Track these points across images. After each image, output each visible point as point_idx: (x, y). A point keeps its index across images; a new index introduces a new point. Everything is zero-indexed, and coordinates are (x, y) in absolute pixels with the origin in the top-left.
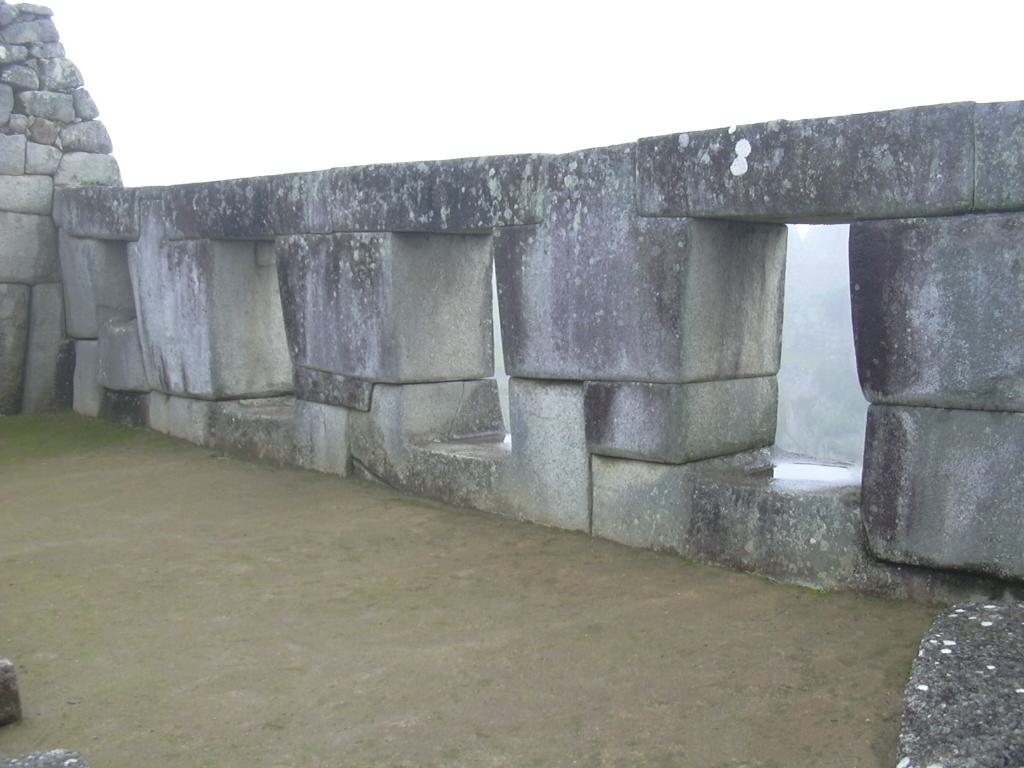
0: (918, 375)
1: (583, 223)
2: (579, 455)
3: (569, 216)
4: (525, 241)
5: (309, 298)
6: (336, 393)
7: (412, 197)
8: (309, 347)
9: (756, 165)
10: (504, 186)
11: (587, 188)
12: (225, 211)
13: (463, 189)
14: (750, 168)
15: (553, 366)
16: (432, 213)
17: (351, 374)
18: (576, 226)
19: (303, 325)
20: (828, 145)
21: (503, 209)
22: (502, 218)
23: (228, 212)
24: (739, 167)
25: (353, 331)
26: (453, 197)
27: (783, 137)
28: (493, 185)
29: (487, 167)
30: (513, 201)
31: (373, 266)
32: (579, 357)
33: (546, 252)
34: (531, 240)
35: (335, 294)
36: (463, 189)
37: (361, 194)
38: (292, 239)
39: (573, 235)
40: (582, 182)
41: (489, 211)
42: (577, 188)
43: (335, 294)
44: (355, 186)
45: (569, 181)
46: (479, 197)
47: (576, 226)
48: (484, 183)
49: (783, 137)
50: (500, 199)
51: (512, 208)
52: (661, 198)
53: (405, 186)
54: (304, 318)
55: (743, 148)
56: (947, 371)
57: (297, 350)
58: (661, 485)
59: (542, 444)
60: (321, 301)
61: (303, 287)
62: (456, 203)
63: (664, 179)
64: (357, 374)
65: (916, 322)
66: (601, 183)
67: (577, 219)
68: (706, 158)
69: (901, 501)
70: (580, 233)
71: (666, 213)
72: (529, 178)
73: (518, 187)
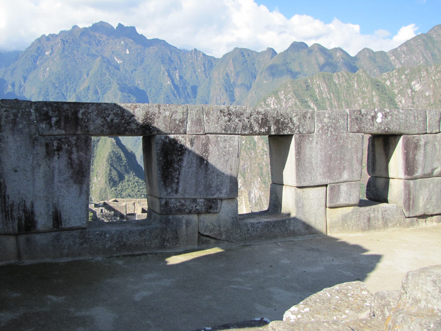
0: (417, 171)
1: (331, 134)
3: (326, 131)
4: (308, 139)
5: (185, 163)
6: (198, 207)
7: (256, 120)
8: (180, 189)
9: (383, 120)
10: (299, 119)
11: (333, 123)
12: (112, 120)
13: (282, 120)
15: (320, 180)
16: (267, 128)
17: (211, 197)
18: (329, 135)
19: (178, 178)
20: (401, 117)
21: (299, 128)
22: (299, 131)
23: (116, 121)
24: (379, 120)
26: (277, 122)
27: (390, 113)
28: (295, 119)
29: (292, 112)
30: (303, 125)
31: (231, 149)
32: (329, 177)
33: (317, 143)
34: (311, 139)
36: (282, 120)
37: (226, 118)
40: (331, 121)
41: (293, 128)
42: (329, 123)
44: (222, 114)
45: (326, 120)
46: (289, 123)
47: (329, 135)
48: (291, 119)
49: (390, 113)
50: (298, 124)
51: (303, 127)
52: (357, 127)
53: (252, 117)
54: (179, 174)
56: (423, 170)
57: (170, 190)
58: (352, 212)
59: (310, 208)
60: (195, 165)
61: (181, 160)
62: (279, 124)
63: (358, 122)
64: (215, 196)
65: (417, 159)
66: (338, 121)
68: (369, 117)
69: (411, 202)
70: (330, 137)
71: (358, 132)
72: (309, 118)
73: (305, 120)
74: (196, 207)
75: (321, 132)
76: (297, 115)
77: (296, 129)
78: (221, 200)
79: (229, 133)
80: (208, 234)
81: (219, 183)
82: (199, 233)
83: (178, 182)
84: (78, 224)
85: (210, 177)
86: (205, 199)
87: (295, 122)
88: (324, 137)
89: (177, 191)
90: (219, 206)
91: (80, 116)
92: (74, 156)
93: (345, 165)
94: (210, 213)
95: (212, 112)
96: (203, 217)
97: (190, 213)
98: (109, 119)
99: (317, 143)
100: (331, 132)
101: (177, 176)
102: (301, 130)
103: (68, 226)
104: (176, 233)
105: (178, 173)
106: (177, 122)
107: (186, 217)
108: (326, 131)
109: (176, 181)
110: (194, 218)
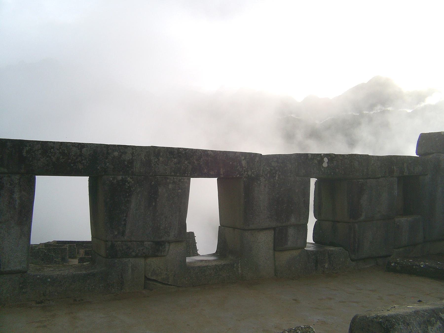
2: (271, 252)
3: (274, 175)
13: (231, 163)
14: (328, 166)
18: (277, 178)
19: (125, 220)
21: (248, 172)
24: (325, 165)
25: (164, 220)
33: (265, 186)
34: (259, 182)
35: (154, 204)
36: (231, 163)
37: (175, 160)
38: (120, 178)
39: (275, 181)
43: (154, 204)
47: (277, 178)
55: (326, 160)
64: (163, 239)
67: (277, 176)
68: (316, 161)
69: (356, 245)
72: (258, 161)
74: (143, 250)
75: (269, 175)
76: (245, 159)
77: (244, 172)
78: (169, 242)
79: (178, 175)
80: (155, 279)
81: (167, 225)
82: (145, 277)
83: (125, 224)
84: (19, 268)
85: (159, 219)
86: (153, 241)
87: (243, 165)
88: (272, 180)
89: (123, 234)
90: (167, 249)
91: (24, 154)
92: (16, 196)
93: (292, 208)
94: (157, 256)
95: (161, 154)
96: (149, 260)
97: (136, 256)
98: (54, 159)
99: (265, 186)
100: (279, 175)
101: (125, 218)
102: (250, 173)
103: (8, 269)
104: (122, 277)
105: (125, 215)
106: (126, 163)
107: (132, 260)
108: (274, 175)
109: (123, 223)
110: (141, 262)
